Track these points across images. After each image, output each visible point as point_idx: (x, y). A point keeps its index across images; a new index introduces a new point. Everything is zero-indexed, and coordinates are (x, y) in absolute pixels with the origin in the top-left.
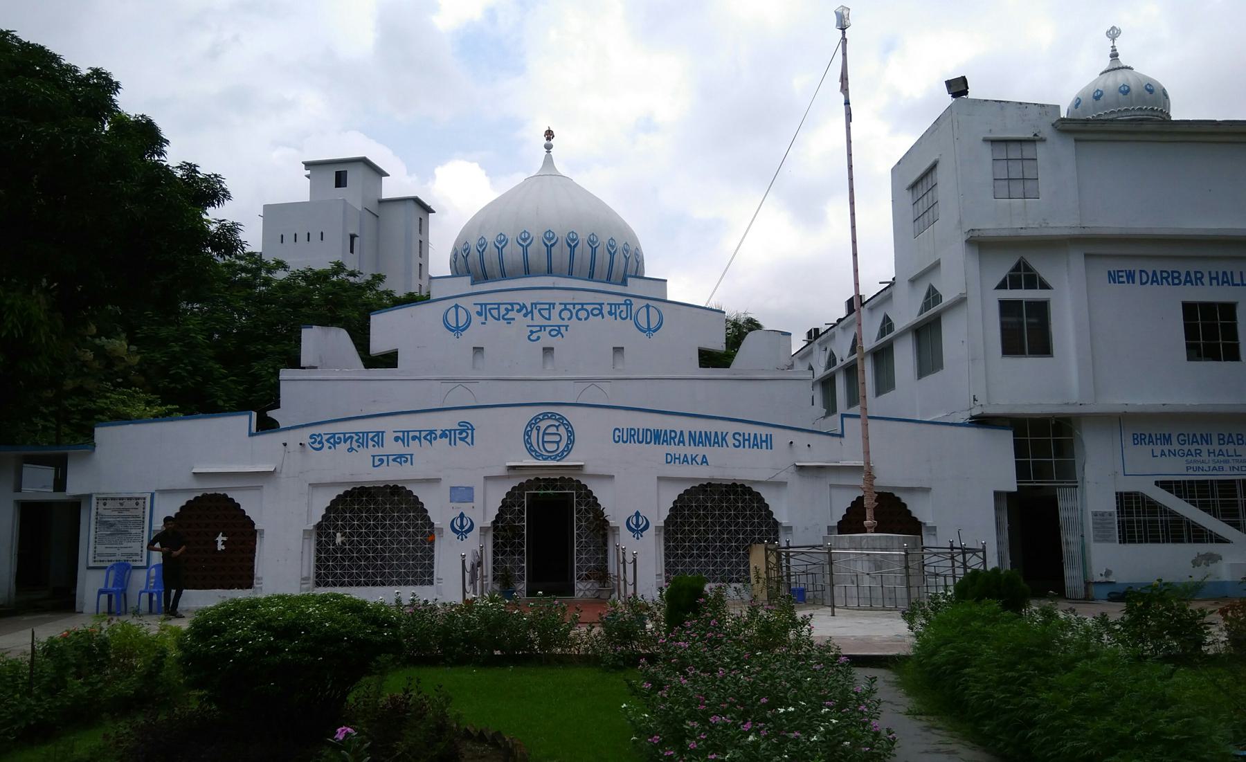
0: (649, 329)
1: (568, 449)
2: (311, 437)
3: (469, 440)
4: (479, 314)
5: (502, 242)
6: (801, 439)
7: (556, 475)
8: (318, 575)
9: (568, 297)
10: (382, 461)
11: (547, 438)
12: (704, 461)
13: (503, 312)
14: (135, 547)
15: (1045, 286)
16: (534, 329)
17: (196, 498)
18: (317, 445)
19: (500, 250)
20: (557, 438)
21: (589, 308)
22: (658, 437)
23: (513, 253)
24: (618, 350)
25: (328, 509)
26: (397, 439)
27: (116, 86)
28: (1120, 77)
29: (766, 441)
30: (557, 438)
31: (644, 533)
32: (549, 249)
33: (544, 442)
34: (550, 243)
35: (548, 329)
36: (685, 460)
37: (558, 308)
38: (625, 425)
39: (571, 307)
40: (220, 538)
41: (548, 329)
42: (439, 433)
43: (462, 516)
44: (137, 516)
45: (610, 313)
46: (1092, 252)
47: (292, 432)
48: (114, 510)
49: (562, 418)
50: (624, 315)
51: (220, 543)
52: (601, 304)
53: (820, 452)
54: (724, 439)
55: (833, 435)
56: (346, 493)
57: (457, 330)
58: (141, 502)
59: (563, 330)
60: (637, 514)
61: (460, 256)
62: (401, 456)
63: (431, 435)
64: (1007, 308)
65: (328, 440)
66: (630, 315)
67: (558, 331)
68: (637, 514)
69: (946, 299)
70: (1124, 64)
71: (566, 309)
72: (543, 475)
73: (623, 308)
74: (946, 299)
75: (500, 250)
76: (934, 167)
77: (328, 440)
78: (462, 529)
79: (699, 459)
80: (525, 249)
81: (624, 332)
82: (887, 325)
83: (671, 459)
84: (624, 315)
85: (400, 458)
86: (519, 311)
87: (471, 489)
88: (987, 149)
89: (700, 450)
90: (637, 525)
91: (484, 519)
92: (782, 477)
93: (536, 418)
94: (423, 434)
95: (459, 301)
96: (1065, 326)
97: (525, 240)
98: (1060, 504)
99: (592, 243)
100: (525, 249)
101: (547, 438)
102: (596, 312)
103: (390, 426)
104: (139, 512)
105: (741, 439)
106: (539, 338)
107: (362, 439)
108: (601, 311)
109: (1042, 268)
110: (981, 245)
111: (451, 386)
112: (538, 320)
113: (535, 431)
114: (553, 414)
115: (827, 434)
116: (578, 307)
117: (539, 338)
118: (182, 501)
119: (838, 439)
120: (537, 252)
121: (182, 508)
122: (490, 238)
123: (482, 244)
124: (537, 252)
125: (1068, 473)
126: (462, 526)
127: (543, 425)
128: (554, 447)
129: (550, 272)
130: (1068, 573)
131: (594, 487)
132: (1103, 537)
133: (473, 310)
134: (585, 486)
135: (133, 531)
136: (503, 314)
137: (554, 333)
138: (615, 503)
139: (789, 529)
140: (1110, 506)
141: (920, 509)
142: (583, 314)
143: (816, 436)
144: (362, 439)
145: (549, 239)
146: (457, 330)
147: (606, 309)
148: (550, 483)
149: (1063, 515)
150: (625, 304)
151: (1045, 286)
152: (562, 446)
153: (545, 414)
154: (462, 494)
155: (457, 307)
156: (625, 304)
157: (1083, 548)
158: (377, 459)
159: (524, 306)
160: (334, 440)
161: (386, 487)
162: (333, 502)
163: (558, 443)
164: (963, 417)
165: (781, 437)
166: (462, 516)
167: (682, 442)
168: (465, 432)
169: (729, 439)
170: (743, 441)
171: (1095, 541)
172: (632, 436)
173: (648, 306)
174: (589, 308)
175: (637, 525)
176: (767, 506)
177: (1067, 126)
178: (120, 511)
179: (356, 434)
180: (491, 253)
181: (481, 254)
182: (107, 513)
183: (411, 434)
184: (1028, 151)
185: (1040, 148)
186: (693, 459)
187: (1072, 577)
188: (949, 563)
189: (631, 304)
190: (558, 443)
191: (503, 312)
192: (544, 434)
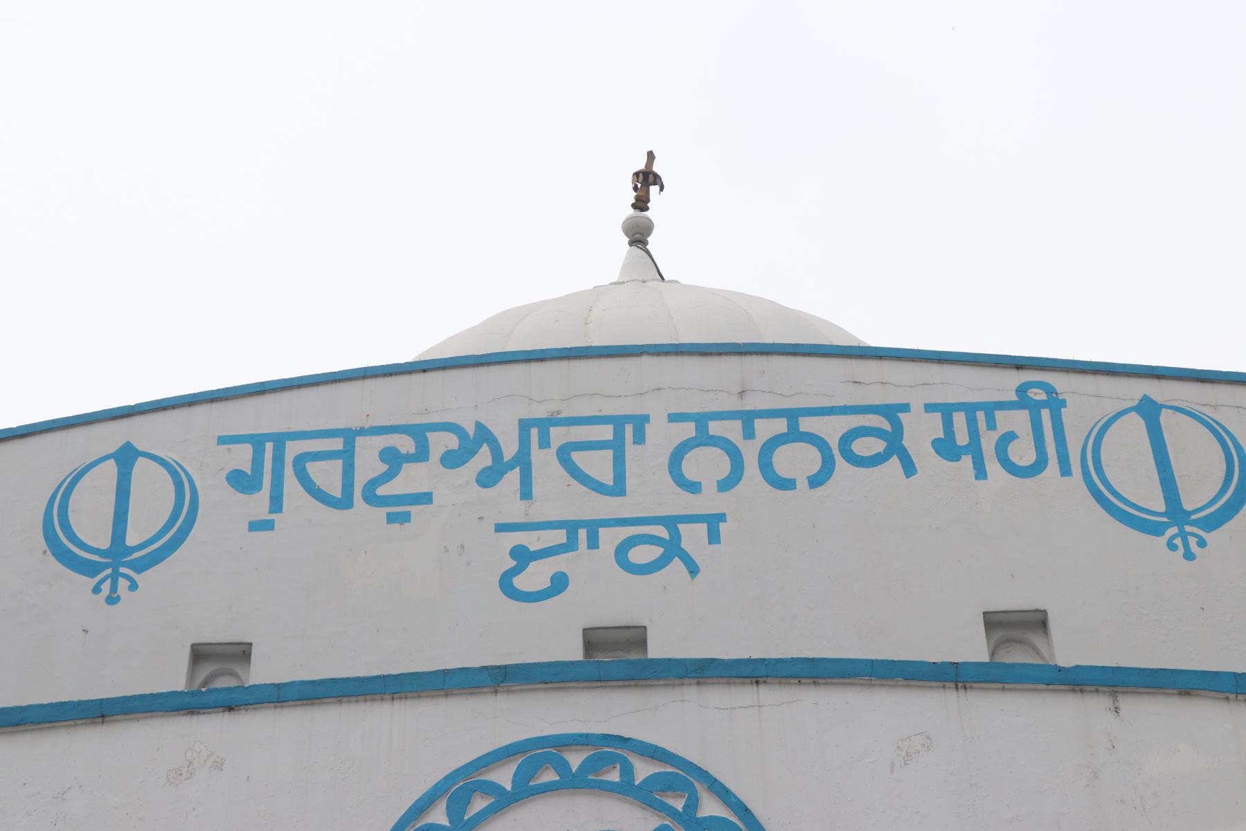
4: (242, 482)
13: (368, 463)
16: (535, 541)
21: (832, 429)
35: (610, 538)
37: (663, 437)
39: (731, 430)
41: (610, 538)
45: (946, 448)
50: (1023, 453)
52: (891, 412)
57: (113, 565)
59: (693, 537)
66: (1051, 453)
71: (703, 439)
73: (1018, 421)
84: (1023, 453)
86: (452, 460)
102: (866, 446)
106: (559, 583)
108: (895, 447)
112: (557, 496)
114: (610, 749)
116: (766, 429)
117: (559, 583)
137: (642, 554)
142: (797, 460)
147: (921, 432)
150: (1022, 400)
155: (126, 457)
156: (1022, 400)
159: (484, 435)
173: (1149, 411)
174: (832, 429)
189: (1055, 403)
191: (368, 463)
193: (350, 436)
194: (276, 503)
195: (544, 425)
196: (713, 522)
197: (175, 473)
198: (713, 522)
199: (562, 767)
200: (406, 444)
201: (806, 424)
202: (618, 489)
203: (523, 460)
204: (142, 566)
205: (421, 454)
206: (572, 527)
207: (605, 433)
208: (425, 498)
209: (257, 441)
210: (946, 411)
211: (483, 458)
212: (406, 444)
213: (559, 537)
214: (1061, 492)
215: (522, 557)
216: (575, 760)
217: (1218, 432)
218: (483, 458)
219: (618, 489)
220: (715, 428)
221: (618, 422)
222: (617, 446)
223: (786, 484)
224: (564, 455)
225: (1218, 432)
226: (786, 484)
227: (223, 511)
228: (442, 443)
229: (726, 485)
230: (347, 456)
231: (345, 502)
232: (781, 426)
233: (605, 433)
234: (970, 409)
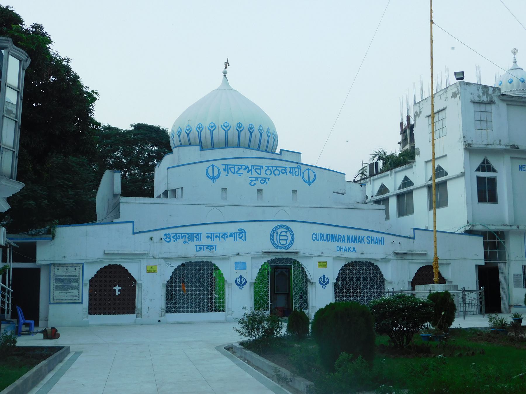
0: (309, 181)
1: (291, 243)
2: (165, 235)
3: (243, 238)
4: (225, 170)
5: (212, 128)
6: (399, 239)
7: (285, 256)
8: (167, 308)
9: (269, 163)
10: (200, 248)
11: (281, 238)
12: (354, 250)
14: (75, 292)
15: (494, 171)
16: (253, 179)
17: (105, 267)
18: (168, 240)
19: (212, 132)
20: (286, 238)
21: (280, 169)
22: (333, 238)
23: (219, 134)
24: (294, 192)
25: (173, 273)
26: (208, 237)
27: (50, 42)
28: (519, 75)
29: (381, 241)
30: (286, 238)
31: (327, 286)
32: (239, 132)
33: (280, 240)
34: (240, 129)
35: (260, 179)
36: (345, 250)
37: (265, 168)
38: (317, 232)
39: (270, 168)
40: (117, 288)
41: (260, 179)
42: (229, 234)
43: (241, 277)
44: (75, 276)
45: (290, 172)
46: (512, 156)
47: (155, 232)
48: (63, 272)
49: (288, 228)
50: (297, 174)
51: (117, 291)
52: (286, 168)
53: (405, 246)
54: (362, 239)
55: (410, 238)
56: (183, 265)
57: (213, 178)
58: (77, 268)
59: (267, 180)
60: (324, 276)
61: (183, 132)
62: (210, 246)
63: (225, 235)
64: (480, 180)
65: (173, 237)
67: (264, 181)
68: (324, 276)
69: (451, 174)
70: (520, 67)
71: (268, 169)
72: (278, 256)
73: (297, 170)
74: (451, 174)
75: (212, 132)
76: (444, 109)
77: (173, 237)
78: (241, 283)
79: (352, 249)
80: (226, 132)
81: (296, 182)
82: (407, 182)
83: (339, 249)
84: (297, 174)
85: (210, 247)
86: (245, 169)
87: (244, 263)
88: (472, 105)
89: (352, 245)
90: (324, 282)
92: (389, 257)
93: (276, 227)
94: (221, 235)
95: (214, 163)
96: (503, 189)
97: (226, 127)
98: (500, 271)
99: (260, 130)
100: (226, 132)
101: (281, 238)
102: (283, 171)
103: (204, 230)
104: (76, 274)
105: (370, 239)
107: (190, 237)
108: (286, 171)
109: (494, 162)
110: (469, 149)
111: (210, 208)
112: (255, 175)
113: (275, 234)
115: (407, 237)
116: (274, 168)
118: (97, 268)
119: (411, 240)
120: (233, 135)
121: (98, 272)
122: (206, 125)
123: (200, 129)
124: (233, 135)
125: (502, 257)
126: (241, 282)
127: (279, 231)
129: (239, 145)
130: (502, 302)
131: (302, 262)
132: (517, 285)
133: (222, 168)
134: (298, 262)
135: (74, 284)
136: (236, 170)
137: (262, 182)
138: (313, 272)
139: (391, 283)
140: (520, 271)
141: (446, 273)
142: (277, 172)
143: (403, 238)
144: (190, 237)
146: (213, 178)
147: (288, 170)
148: (281, 260)
149: (500, 275)
150: (298, 168)
151: (494, 171)
154: (243, 266)
155: (213, 166)
156: (298, 168)
157: (508, 290)
158: (198, 247)
159: (248, 167)
160: (176, 237)
161: (202, 262)
162: (176, 270)
163: (286, 240)
164: (462, 230)
165: (388, 239)
166: (241, 277)
167: (344, 241)
168: (241, 234)
169: (365, 239)
170: (371, 241)
171: (514, 287)
172: (321, 237)
173: (308, 170)
174: (280, 169)
175: (324, 282)
176: (380, 272)
177: (505, 98)
178: (67, 273)
179: (188, 234)
180: (206, 134)
181: (200, 133)
182: (59, 274)
183: (215, 235)
184: (488, 108)
185: (493, 106)
186: (349, 249)
187: (504, 303)
188: (466, 297)
189: (301, 168)
190: (286, 240)
191: (237, 169)
192: (280, 236)
193: (235, 165)
194: (228, 173)
195: (254, 166)
196: (269, 178)
197: (218, 168)
198: (269, 178)
200: (240, 167)
201: (278, 168)
202: (260, 174)
203: (251, 170)
204: (216, 179)
205: (242, 169)
206: (256, 178)
207: (259, 168)
208: (242, 174)
209: (226, 165)
210: (290, 168)
211: (247, 170)
212: (240, 167)
213: (255, 179)
214: (300, 178)
215: (252, 181)
217: (314, 172)
218: (247, 170)
219: (260, 174)
220: (270, 168)
221: (260, 166)
222: (260, 169)
223: (275, 175)
224: (255, 169)
225: (314, 172)
226: (275, 175)
227: (223, 173)
228: (244, 167)
229: (270, 174)
230: (234, 168)
231: (234, 173)
232: (275, 168)
233: (259, 168)
234: (293, 168)
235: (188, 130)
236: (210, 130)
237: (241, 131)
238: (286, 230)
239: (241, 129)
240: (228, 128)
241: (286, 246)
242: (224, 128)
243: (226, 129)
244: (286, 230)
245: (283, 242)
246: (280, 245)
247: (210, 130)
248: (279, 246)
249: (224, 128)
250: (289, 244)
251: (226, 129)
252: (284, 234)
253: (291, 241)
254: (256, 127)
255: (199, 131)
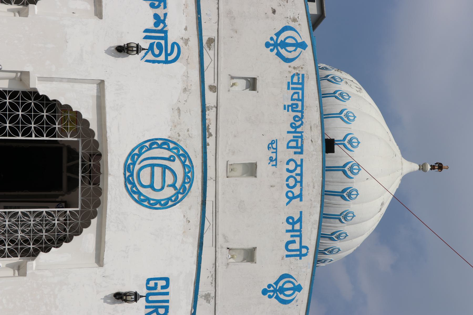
11: (158, 171)
19: (338, 115)
24: (250, 255)
30: (157, 185)
33: (152, 166)
61: (327, 73)
75: (338, 115)
91: (42, 79)
93: (186, 155)
101: (158, 171)
113: (166, 154)
114: (191, 181)
127: (177, 166)
128: (146, 180)
145: (351, 169)
152: (147, 192)
153: (192, 167)
163: (151, 186)
190: (151, 186)
192: (165, 168)
199: (189, 172)
216: (189, 175)
235: (333, 77)
236: (341, 112)
237: (345, 172)
238: (178, 185)
239: (349, 173)
240: (349, 146)
241: (134, 185)
242: (348, 138)
243: (346, 142)
244: (178, 185)
245: (145, 177)
246: (137, 167)
247: (341, 112)
248: (134, 164)
249: (348, 138)
250: (140, 193)
251: (346, 142)
252: (169, 179)
253: (148, 199)
254: (351, 206)
255: (337, 95)
